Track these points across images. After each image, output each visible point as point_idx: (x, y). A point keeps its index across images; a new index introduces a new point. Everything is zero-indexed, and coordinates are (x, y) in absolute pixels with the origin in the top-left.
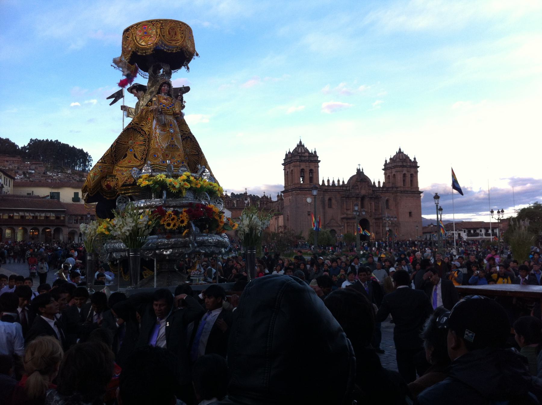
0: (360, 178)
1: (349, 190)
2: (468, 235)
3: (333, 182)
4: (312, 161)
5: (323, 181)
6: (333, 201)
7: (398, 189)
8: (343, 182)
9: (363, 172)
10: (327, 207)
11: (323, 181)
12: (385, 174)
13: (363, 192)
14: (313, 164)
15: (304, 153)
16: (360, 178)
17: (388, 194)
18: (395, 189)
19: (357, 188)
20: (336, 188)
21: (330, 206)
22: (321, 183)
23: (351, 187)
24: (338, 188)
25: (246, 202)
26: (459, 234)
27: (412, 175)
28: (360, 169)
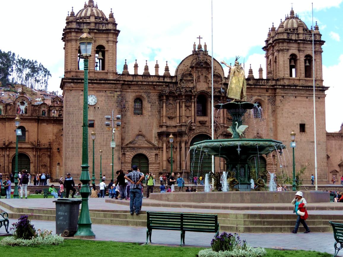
0: (200, 62)
1: (176, 83)
3: (146, 68)
4: (107, 32)
5: (126, 67)
6: (146, 105)
7: (279, 83)
8: (167, 69)
9: (205, 53)
10: (129, 113)
11: (126, 67)
12: (267, 57)
13: (201, 87)
14: (104, 36)
15: (89, 18)
16: (200, 62)
17: (257, 91)
18: (274, 83)
19: (189, 78)
20: (152, 79)
21: (139, 111)
22: (120, 71)
23: (179, 78)
24: (156, 79)
25: (23, 108)
27: (308, 58)
28: (200, 47)
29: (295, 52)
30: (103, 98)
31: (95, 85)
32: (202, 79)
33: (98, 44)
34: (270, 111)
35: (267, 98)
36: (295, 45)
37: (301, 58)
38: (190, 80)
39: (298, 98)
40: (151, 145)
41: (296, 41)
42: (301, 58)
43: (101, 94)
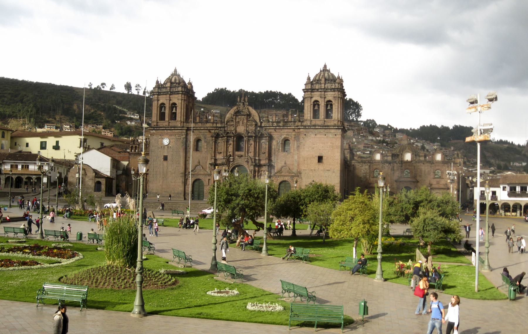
2: (510, 195)
17: (286, 130)
26: (494, 193)
29: (318, 99)
30: (174, 140)
31: (169, 131)
32: (241, 123)
33: (171, 102)
34: (295, 146)
35: (293, 136)
36: (318, 93)
37: (322, 104)
38: (232, 125)
39: (318, 136)
40: (206, 173)
41: (318, 90)
42: (322, 104)
43: (172, 137)
